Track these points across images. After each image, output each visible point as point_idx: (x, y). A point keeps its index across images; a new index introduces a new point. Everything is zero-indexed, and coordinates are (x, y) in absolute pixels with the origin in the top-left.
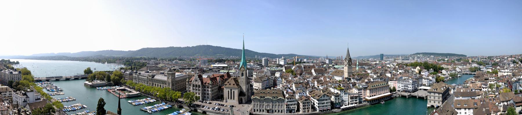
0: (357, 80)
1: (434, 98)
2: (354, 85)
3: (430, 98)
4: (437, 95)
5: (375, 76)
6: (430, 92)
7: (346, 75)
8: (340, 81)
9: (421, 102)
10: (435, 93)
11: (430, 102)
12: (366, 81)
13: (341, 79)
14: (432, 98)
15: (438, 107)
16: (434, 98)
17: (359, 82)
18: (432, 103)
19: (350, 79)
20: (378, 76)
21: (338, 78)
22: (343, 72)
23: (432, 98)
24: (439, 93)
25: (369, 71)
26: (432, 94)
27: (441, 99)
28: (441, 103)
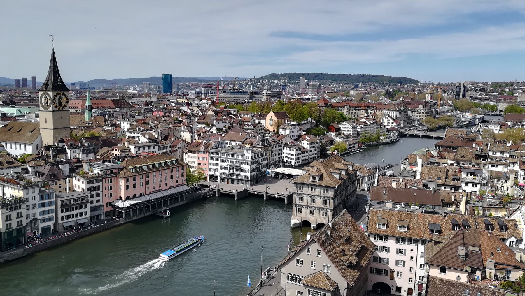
0: (86, 152)
1: (312, 201)
2: (75, 168)
3: (301, 199)
4: (319, 191)
5: (143, 140)
6: (301, 185)
7: (48, 137)
8: (24, 160)
9: (273, 214)
10: (314, 186)
11: (300, 211)
12: (116, 152)
13: (29, 150)
14: (306, 200)
15: (320, 226)
16: (312, 201)
17: (91, 156)
18: (305, 215)
19: (62, 151)
20: (152, 139)
21: (16, 150)
22: (35, 129)
23: (306, 200)
24: (326, 188)
25: (125, 125)
26: (307, 190)
27: (330, 204)
28: (330, 214)
